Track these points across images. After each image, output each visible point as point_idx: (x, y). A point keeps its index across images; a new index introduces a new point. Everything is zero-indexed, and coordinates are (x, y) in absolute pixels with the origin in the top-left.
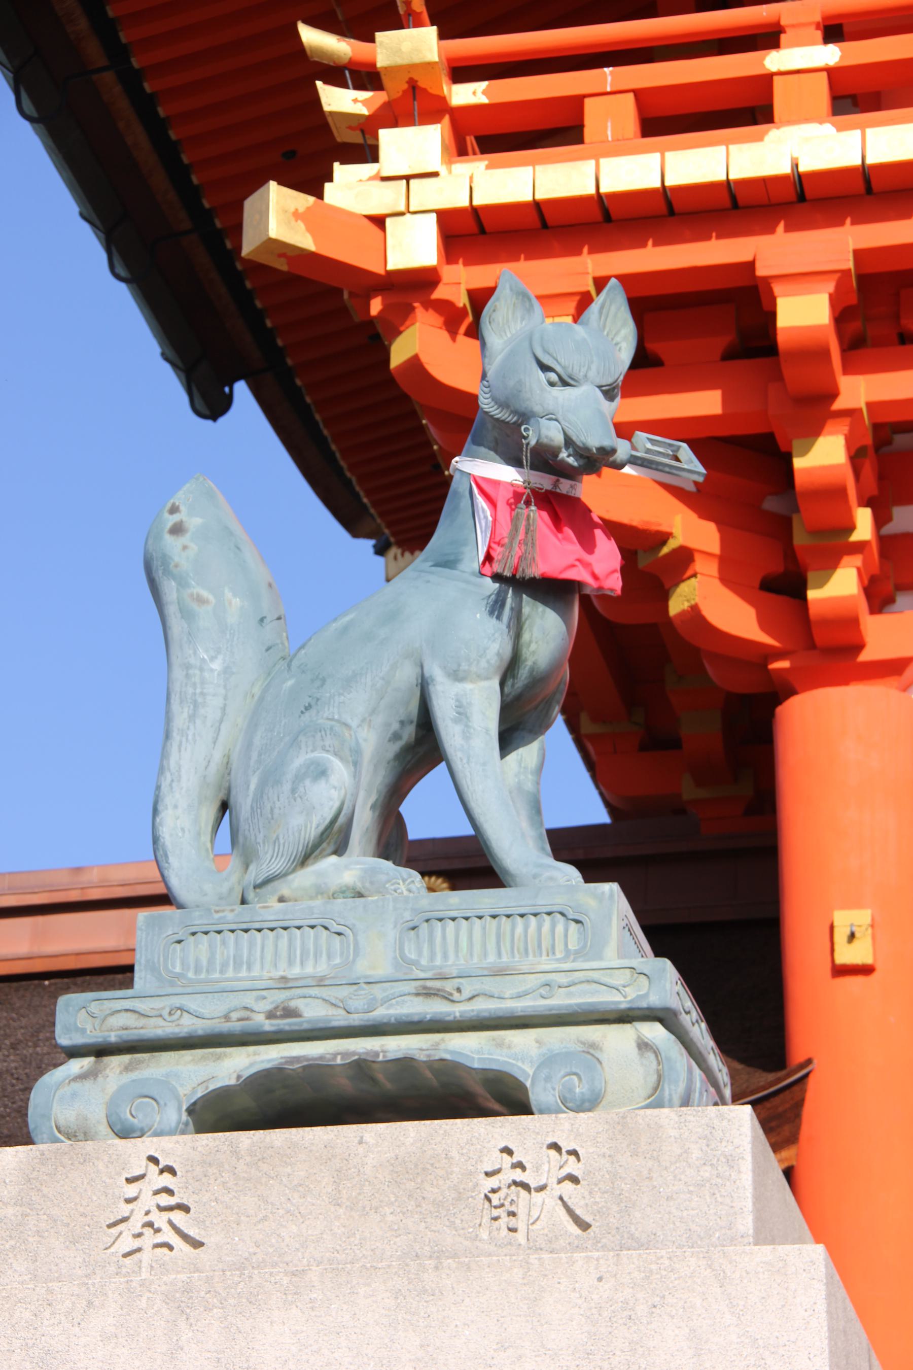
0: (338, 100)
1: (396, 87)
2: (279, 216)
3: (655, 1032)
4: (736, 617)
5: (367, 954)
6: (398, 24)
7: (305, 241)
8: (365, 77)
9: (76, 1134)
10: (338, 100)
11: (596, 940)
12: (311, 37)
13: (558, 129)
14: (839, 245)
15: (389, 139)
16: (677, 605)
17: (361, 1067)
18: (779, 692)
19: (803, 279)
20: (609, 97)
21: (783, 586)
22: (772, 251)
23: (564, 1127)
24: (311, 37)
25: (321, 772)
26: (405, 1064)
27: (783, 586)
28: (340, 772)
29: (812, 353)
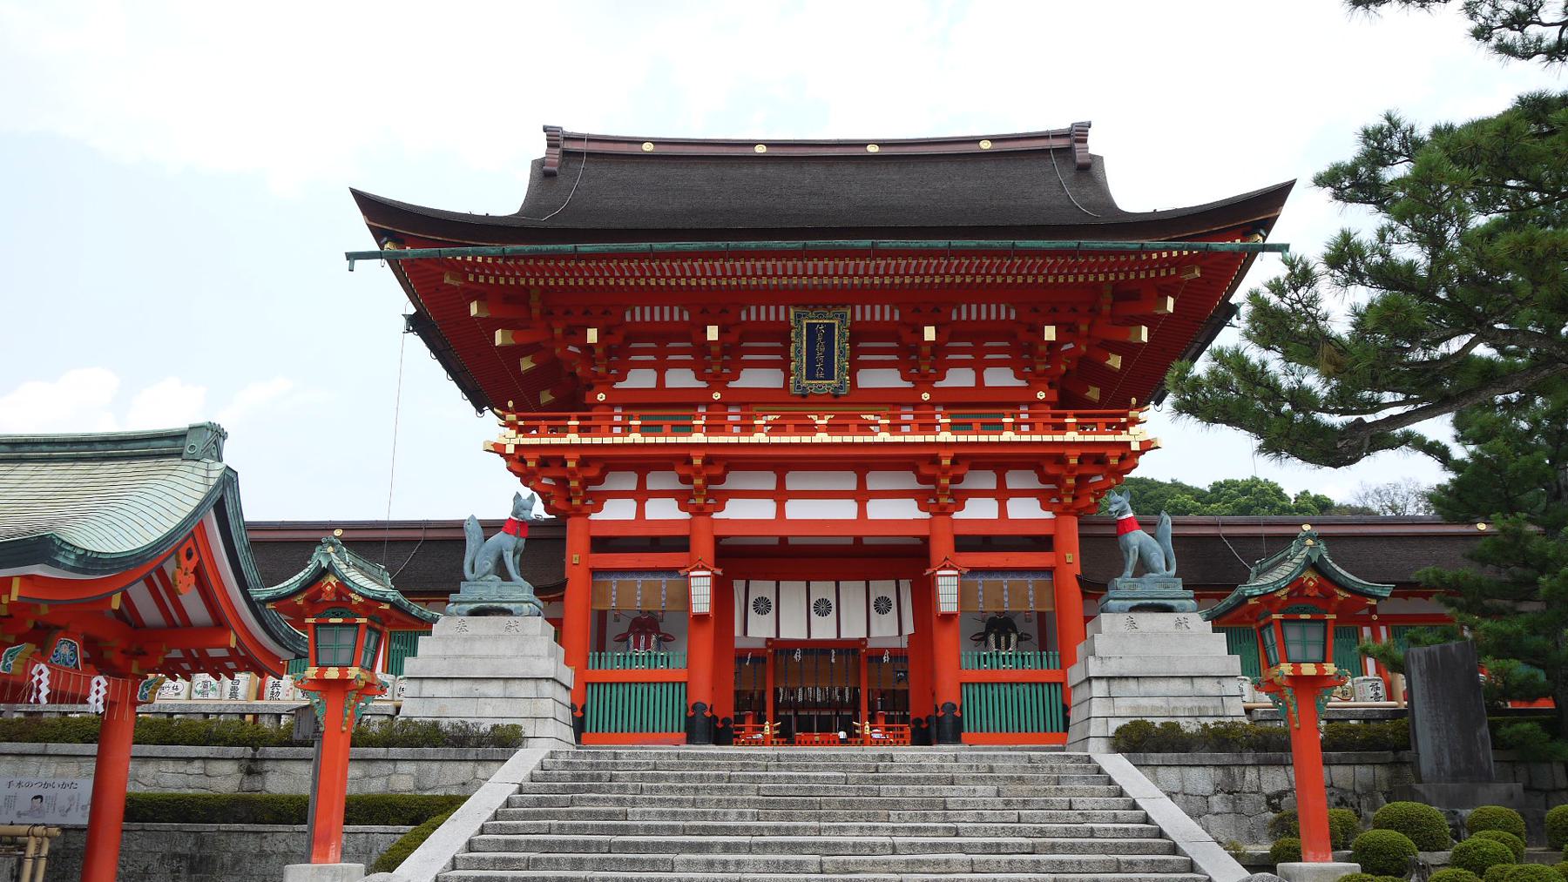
9: (451, 615)
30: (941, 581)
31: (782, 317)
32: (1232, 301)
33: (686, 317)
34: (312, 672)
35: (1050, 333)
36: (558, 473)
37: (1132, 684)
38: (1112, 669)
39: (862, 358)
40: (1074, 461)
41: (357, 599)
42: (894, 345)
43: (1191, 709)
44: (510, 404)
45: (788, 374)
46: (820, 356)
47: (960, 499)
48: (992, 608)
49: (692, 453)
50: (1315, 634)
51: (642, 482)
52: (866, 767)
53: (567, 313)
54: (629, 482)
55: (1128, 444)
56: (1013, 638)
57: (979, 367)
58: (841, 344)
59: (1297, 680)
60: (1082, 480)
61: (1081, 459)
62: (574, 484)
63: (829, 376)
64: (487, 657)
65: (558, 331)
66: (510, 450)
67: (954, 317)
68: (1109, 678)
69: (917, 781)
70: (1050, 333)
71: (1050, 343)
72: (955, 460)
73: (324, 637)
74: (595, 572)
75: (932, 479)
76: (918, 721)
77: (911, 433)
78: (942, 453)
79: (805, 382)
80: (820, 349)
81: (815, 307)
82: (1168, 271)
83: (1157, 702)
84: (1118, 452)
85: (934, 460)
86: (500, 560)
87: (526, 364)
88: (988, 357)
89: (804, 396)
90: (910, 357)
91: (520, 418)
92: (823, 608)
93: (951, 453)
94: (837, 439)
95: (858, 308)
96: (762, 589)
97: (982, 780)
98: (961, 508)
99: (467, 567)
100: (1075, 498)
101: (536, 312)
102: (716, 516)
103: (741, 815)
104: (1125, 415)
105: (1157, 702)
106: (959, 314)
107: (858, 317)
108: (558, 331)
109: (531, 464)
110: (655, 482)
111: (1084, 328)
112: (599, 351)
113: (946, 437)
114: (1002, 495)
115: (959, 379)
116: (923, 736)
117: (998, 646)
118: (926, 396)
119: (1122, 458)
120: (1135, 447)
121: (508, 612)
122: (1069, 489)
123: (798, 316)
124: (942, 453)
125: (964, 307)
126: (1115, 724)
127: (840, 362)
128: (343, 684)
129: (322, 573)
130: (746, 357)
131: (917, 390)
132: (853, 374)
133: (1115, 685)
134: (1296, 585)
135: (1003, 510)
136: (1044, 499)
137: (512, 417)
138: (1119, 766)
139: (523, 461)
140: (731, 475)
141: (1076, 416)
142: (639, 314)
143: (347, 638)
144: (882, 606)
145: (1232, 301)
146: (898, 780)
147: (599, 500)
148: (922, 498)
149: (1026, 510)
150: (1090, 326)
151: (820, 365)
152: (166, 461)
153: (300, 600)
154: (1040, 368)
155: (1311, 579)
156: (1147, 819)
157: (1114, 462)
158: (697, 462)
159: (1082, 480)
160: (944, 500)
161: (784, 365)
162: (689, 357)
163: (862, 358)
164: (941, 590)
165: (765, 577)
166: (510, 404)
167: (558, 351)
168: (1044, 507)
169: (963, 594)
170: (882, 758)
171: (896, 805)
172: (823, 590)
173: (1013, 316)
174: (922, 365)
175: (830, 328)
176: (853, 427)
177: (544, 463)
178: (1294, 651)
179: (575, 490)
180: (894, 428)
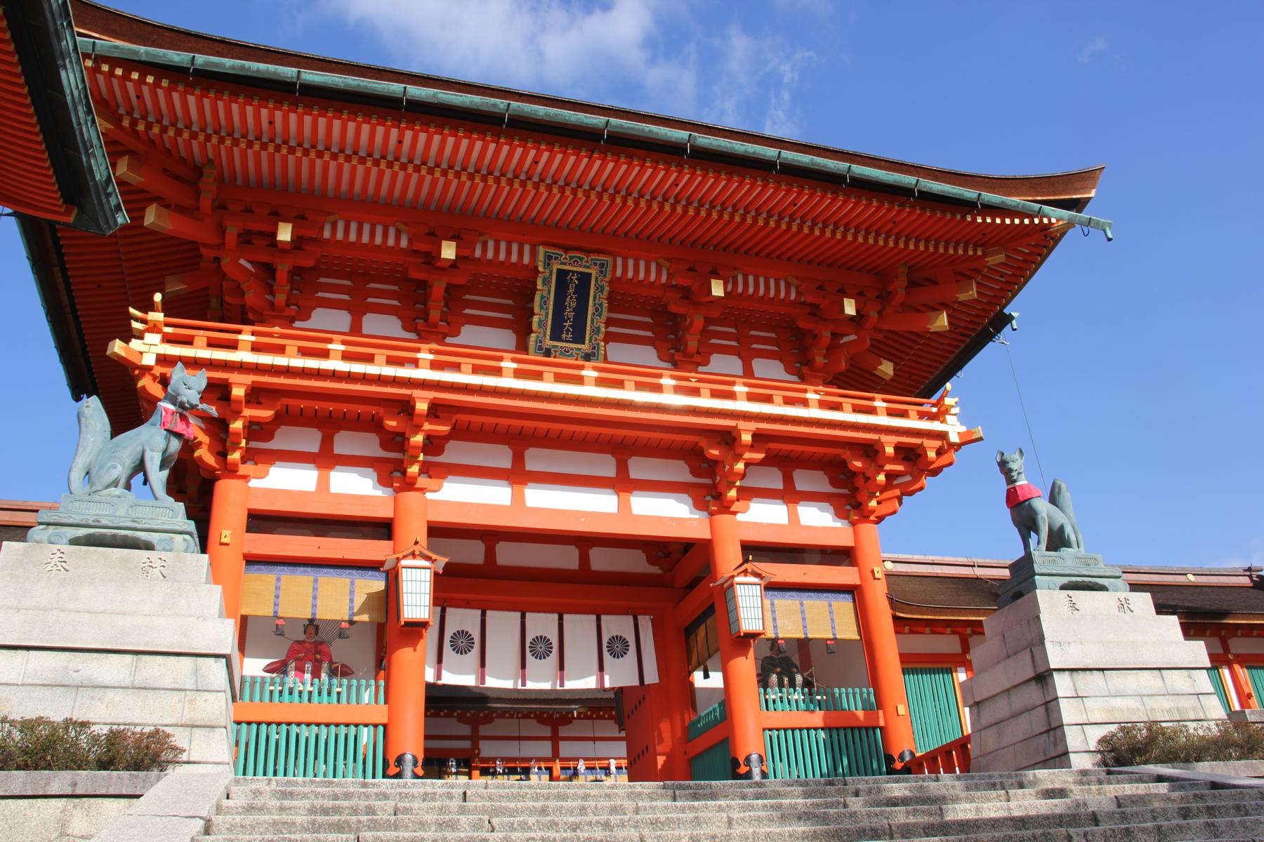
0: (135, 325)
1: (151, 325)
2: (117, 347)
3: (188, 537)
4: (210, 459)
5: (119, 509)
6: (153, 311)
7: (123, 354)
8: (144, 321)
10: (135, 325)
11: (175, 514)
12: (132, 310)
13: (188, 342)
14: (249, 379)
15: (147, 335)
16: (196, 454)
17: (114, 536)
18: (217, 478)
19: (240, 385)
20: (201, 337)
21: (222, 455)
22: (233, 377)
23: (163, 555)
24: (132, 310)
25: (115, 467)
26: (126, 537)
27: (222, 455)
28: (120, 468)
29: (238, 402)
30: (739, 590)
31: (526, 260)
32: (1006, 311)
33: (404, 243)
35: (850, 308)
39: (611, 329)
40: (890, 450)
42: (648, 320)
43: (1169, 711)
44: (158, 297)
46: (569, 313)
49: (416, 393)
51: (327, 442)
53: (248, 211)
54: (310, 441)
61: (898, 447)
64: (104, 612)
65: (232, 231)
70: (850, 308)
74: (253, 561)
79: (548, 343)
80: (571, 303)
81: (567, 249)
82: (975, 251)
84: (938, 444)
86: (140, 467)
91: (167, 325)
92: (540, 648)
95: (619, 261)
100: (879, 503)
102: (429, 496)
105: (1133, 703)
107: (619, 273)
108: (232, 231)
110: (345, 443)
112: (283, 268)
119: (940, 452)
121: (149, 546)
125: (740, 278)
130: (468, 311)
137: (158, 316)
140: (451, 446)
141: (884, 400)
142: (337, 231)
144: (617, 647)
145: (1006, 311)
150: (880, 312)
157: (931, 454)
158: (422, 406)
162: (395, 303)
163: (611, 329)
164: (741, 602)
165: (467, 605)
166: (158, 297)
167: (225, 262)
172: (542, 624)
175: (585, 279)
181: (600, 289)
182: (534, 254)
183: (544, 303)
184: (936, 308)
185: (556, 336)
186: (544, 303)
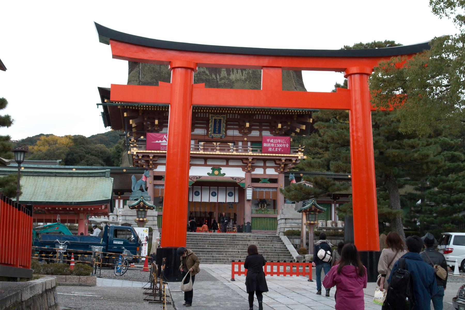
10: (131, 145)
30: (247, 191)
31: (207, 116)
34: (137, 219)
35: (280, 126)
36: (147, 159)
37: (291, 221)
38: (286, 216)
39: (229, 127)
40: (283, 161)
41: (147, 207)
45: (208, 131)
46: (217, 127)
47: (253, 168)
48: (261, 198)
50: (314, 216)
52: (231, 238)
55: (298, 157)
56: (265, 205)
57: (261, 130)
58: (223, 124)
59: (310, 224)
60: (286, 165)
61: (285, 160)
62: (151, 162)
63: (219, 132)
66: (135, 153)
67: (254, 118)
68: (286, 219)
69: (242, 240)
70: (280, 126)
71: (280, 129)
72: (253, 159)
73: (140, 213)
74: (155, 185)
75: (246, 163)
76: (239, 226)
77: (241, 152)
78: (249, 158)
80: (217, 125)
83: (296, 225)
85: (247, 159)
86: (141, 186)
87: (134, 125)
88: (263, 128)
89: (212, 138)
90: (241, 128)
93: (252, 158)
94: (222, 153)
96: (197, 188)
97: (256, 241)
98: (254, 170)
99: (132, 188)
100: (284, 169)
101: (140, 114)
103: (208, 246)
104: (298, 149)
106: (256, 117)
108: (146, 119)
109: (140, 157)
111: (289, 123)
113: (250, 153)
114: (265, 168)
115: (255, 133)
116: (240, 230)
117: (261, 207)
118: (245, 139)
119: (296, 160)
120: (300, 158)
122: (282, 167)
123: (212, 117)
124: (249, 158)
126: (286, 229)
127: (223, 129)
128: (143, 221)
129: (140, 201)
131: (243, 137)
132: (226, 132)
133: (287, 221)
134: (310, 208)
135: (265, 172)
136: (276, 169)
137: (135, 145)
138: (285, 239)
139: (138, 156)
143: (143, 213)
144: (231, 194)
146: (237, 240)
147: (156, 165)
148: (244, 168)
149: (271, 172)
151: (217, 130)
152: (102, 178)
153: (136, 206)
154: (277, 132)
155: (313, 207)
156: (287, 248)
157: (294, 161)
159: (286, 165)
160: (249, 169)
161: (207, 128)
164: (247, 193)
167: (145, 123)
168: (276, 171)
169: (254, 194)
170: (234, 236)
171: (238, 245)
172: (214, 189)
173: (270, 118)
174: (245, 132)
175: (220, 120)
176: (226, 150)
177: (143, 156)
178: (310, 219)
179: (151, 164)
180: (237, 150)
181: (223, 122)
182: (209, 115)
183: (211, 126)
184: (303, 123)
185: (214, 132)
186: (211, 126)
